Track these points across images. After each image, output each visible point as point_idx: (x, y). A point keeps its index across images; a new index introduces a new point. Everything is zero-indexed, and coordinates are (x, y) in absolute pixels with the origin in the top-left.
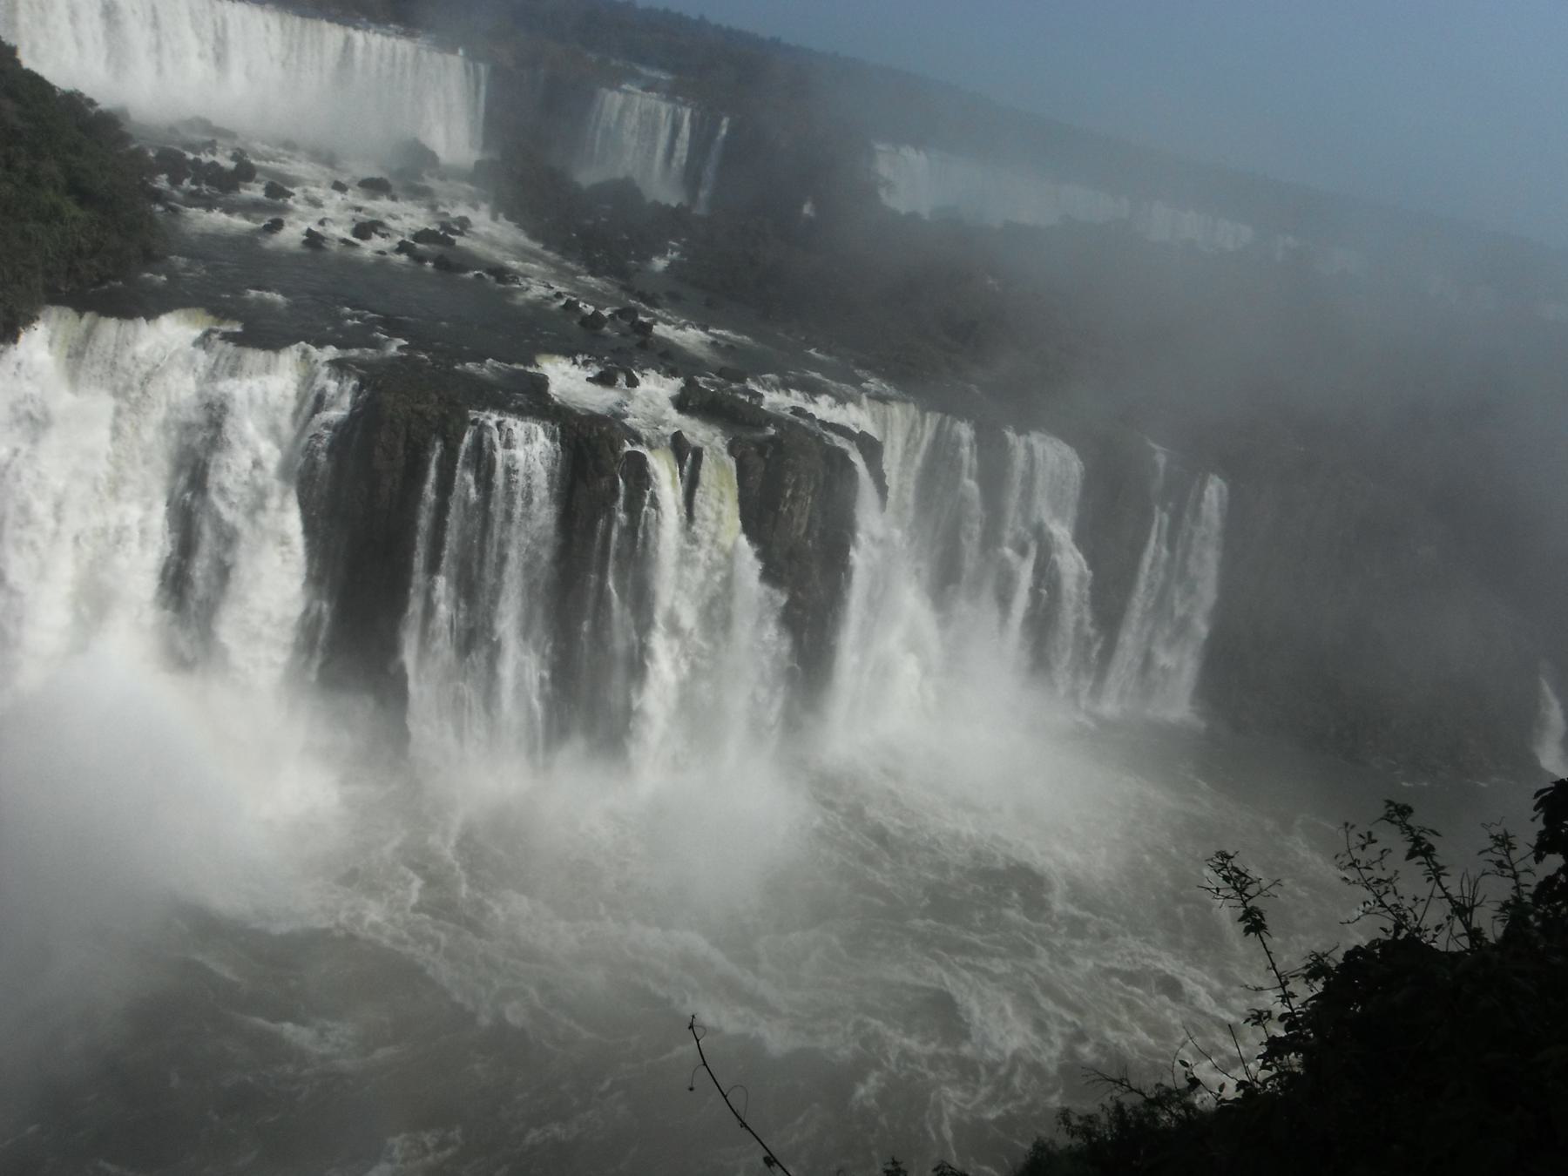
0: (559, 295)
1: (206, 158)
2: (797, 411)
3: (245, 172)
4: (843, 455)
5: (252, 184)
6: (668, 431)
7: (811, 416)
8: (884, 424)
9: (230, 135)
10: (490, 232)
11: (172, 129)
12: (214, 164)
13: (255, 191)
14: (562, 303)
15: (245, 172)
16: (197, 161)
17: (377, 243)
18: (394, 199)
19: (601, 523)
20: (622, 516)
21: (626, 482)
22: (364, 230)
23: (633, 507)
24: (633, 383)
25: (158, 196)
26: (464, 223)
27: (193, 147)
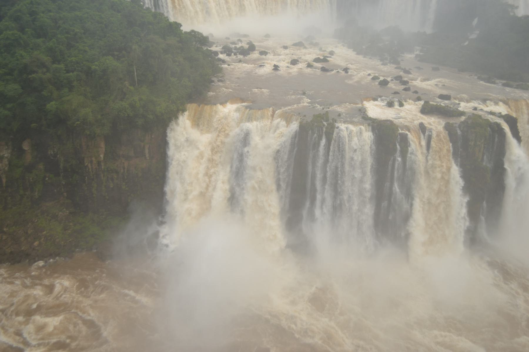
0: (369, 75)
1: (238, 46)
2: (475, 109)
3: (252, 48)
4: (498, 125)
5: (254, 52)
6: (417, 123)
7: (482, 110)
8: (517, 110)
9: (245, 36)
10: (342, 55)
11: (228, 38)
12: (242, 47)
13: (255, 55)
14: (371, 77)
15: (252, 48)
16: (235, 47)
17: (300, 65)
18: (305, 48)
19: (390, 163)
20: (399, 159)
21: (400, 145)
22: (294, 62)
23: (404, 153)
24: (401, 105)
25: (224, 62)
26: (332, 53)
27: (233, 43)
